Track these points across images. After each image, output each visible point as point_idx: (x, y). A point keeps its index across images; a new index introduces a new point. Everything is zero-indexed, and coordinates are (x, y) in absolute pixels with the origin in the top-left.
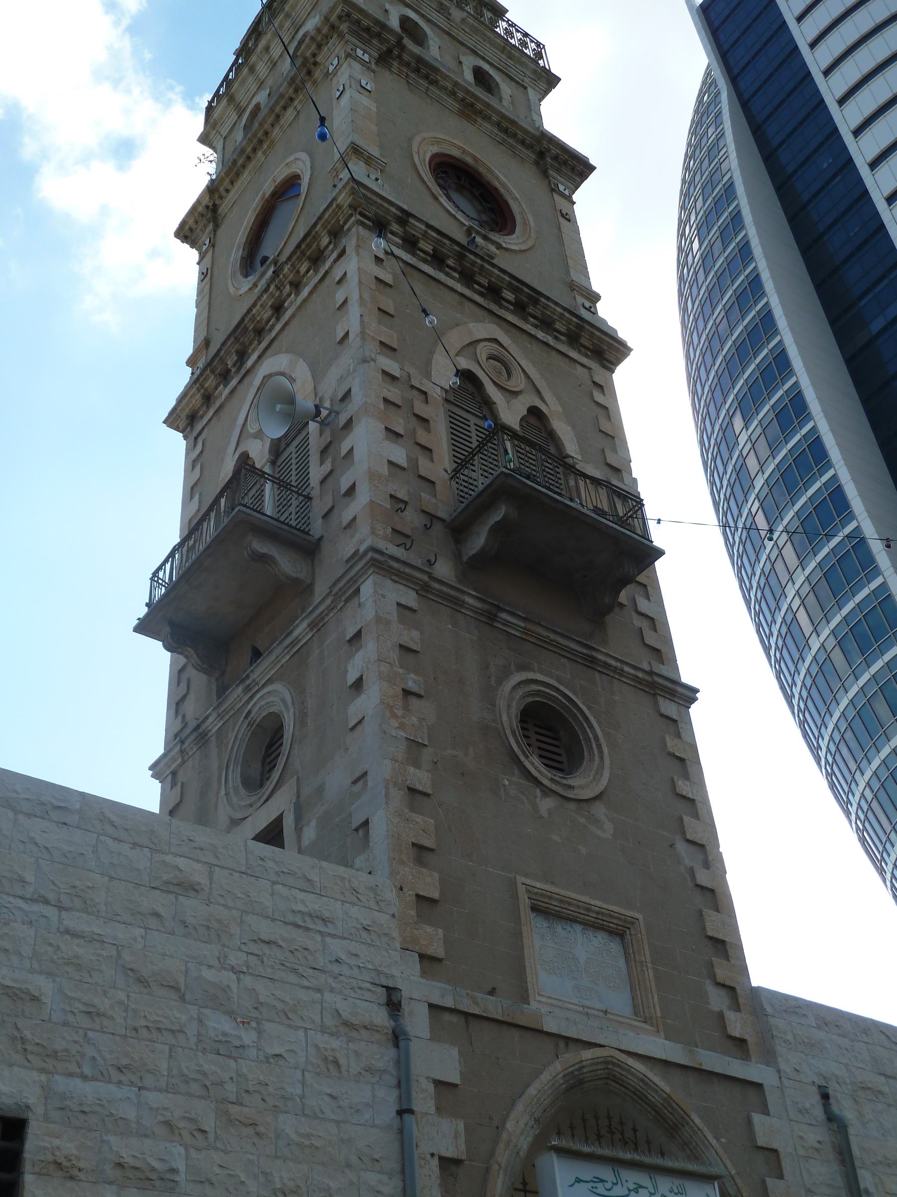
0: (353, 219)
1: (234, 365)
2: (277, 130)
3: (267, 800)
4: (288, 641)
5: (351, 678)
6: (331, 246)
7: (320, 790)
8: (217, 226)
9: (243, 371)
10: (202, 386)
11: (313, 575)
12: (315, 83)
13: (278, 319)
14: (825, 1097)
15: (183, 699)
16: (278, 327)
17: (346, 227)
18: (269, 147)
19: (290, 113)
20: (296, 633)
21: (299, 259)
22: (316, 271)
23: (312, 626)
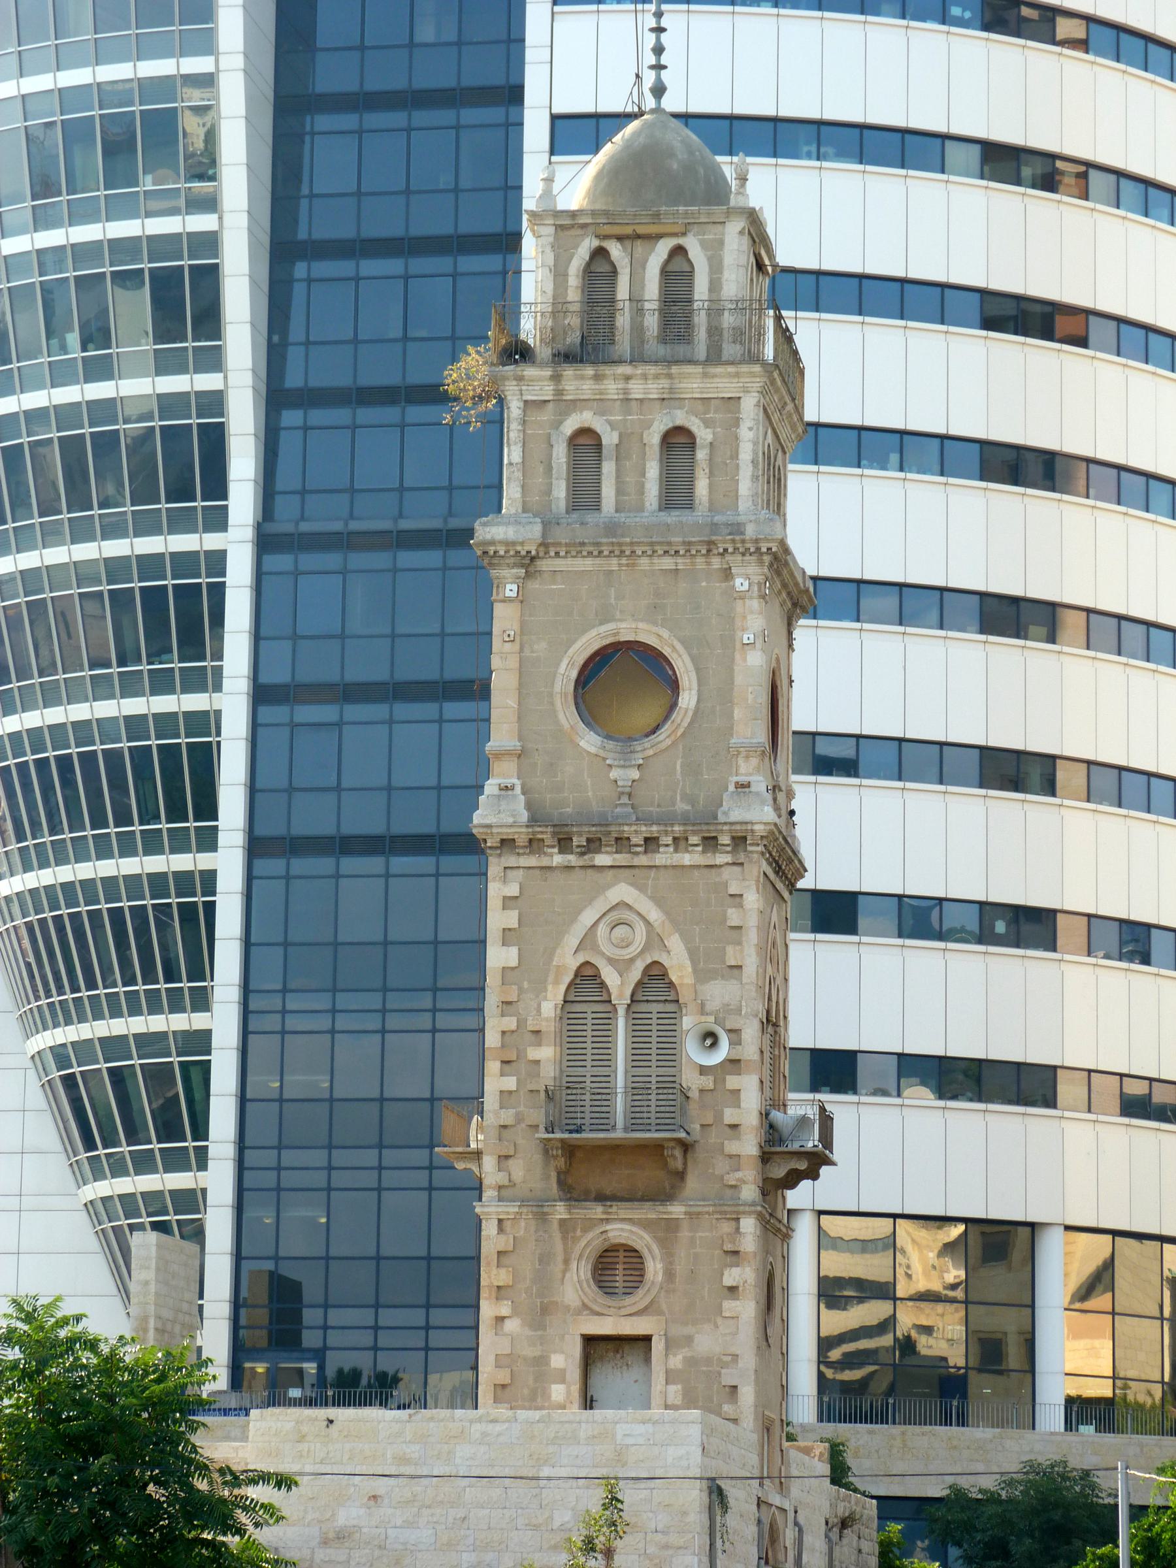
0: (760, 848)
1: (578, 846)
2: (644, 561)
3: (630, 1315)
4: (661, 1208)
5: (728, 1281)
6: (729, 849)
7: (689, 1340)
8: (528, 575)
9: (586, 860)
10: (534, 833)
11: (685, 1164)
12: (708, 563)
13: (646, 852)
14: (796, 1512)
15: (507, 1157)
16: (643, 860)
17: (750, 848)
18: (627, 565)
19: (667, 563)
20: (670, 1208)
21: (694, 833)
22: (704, 852)
23: (686, 1213)
